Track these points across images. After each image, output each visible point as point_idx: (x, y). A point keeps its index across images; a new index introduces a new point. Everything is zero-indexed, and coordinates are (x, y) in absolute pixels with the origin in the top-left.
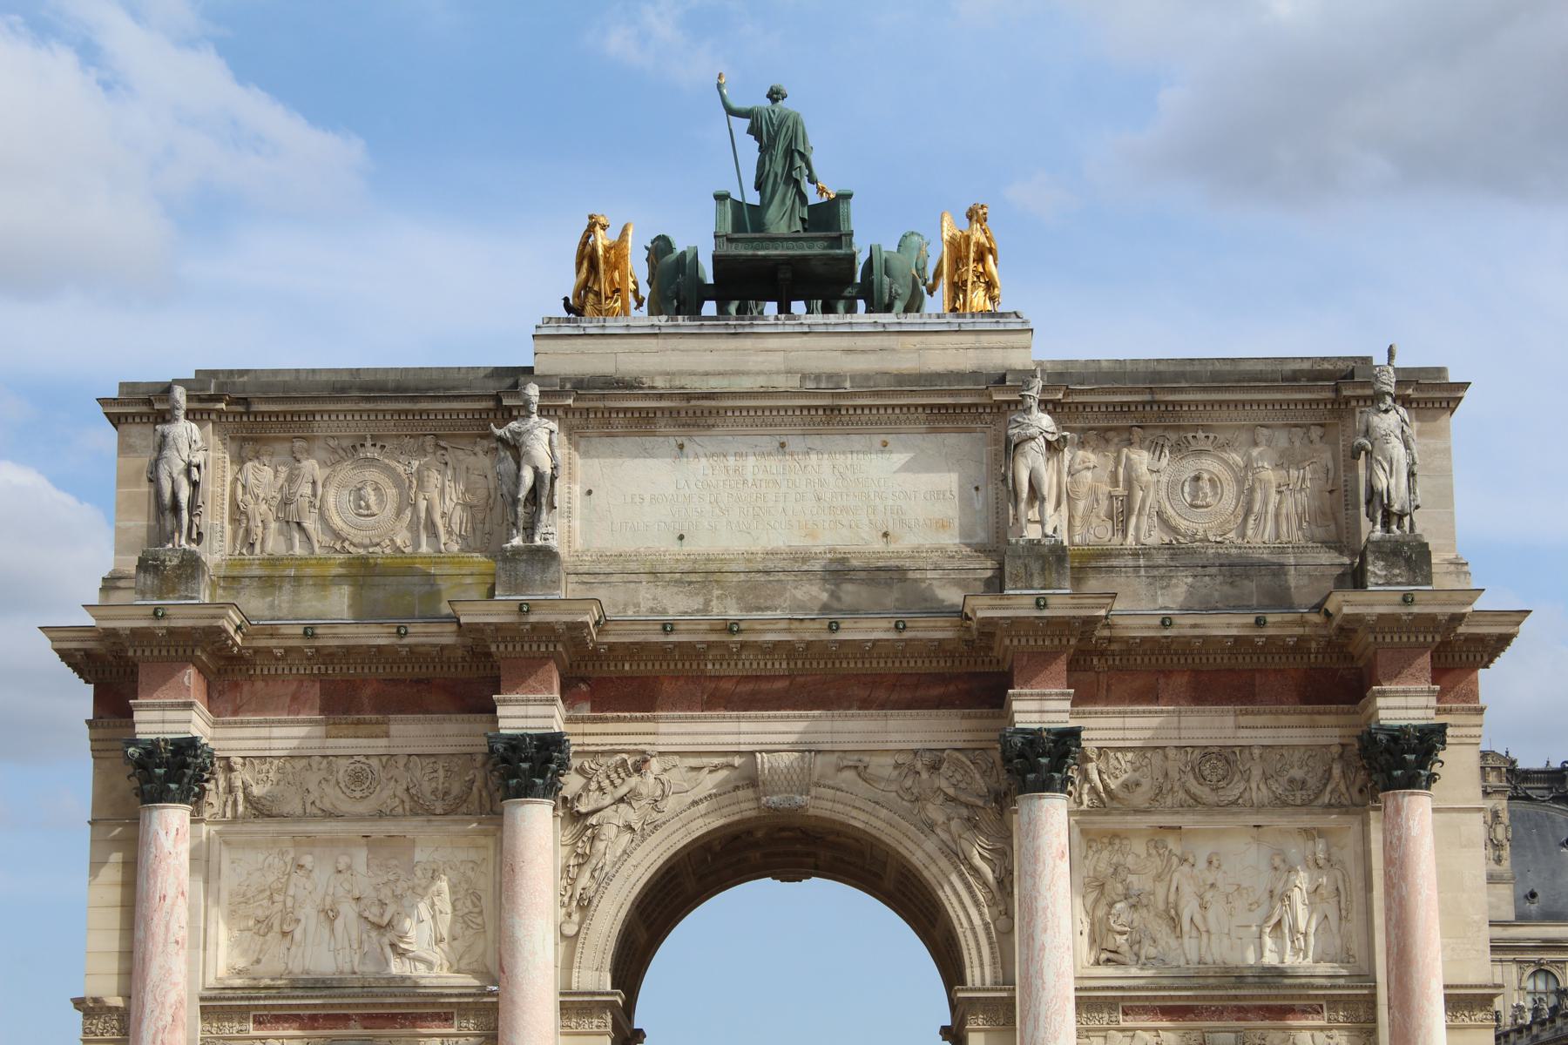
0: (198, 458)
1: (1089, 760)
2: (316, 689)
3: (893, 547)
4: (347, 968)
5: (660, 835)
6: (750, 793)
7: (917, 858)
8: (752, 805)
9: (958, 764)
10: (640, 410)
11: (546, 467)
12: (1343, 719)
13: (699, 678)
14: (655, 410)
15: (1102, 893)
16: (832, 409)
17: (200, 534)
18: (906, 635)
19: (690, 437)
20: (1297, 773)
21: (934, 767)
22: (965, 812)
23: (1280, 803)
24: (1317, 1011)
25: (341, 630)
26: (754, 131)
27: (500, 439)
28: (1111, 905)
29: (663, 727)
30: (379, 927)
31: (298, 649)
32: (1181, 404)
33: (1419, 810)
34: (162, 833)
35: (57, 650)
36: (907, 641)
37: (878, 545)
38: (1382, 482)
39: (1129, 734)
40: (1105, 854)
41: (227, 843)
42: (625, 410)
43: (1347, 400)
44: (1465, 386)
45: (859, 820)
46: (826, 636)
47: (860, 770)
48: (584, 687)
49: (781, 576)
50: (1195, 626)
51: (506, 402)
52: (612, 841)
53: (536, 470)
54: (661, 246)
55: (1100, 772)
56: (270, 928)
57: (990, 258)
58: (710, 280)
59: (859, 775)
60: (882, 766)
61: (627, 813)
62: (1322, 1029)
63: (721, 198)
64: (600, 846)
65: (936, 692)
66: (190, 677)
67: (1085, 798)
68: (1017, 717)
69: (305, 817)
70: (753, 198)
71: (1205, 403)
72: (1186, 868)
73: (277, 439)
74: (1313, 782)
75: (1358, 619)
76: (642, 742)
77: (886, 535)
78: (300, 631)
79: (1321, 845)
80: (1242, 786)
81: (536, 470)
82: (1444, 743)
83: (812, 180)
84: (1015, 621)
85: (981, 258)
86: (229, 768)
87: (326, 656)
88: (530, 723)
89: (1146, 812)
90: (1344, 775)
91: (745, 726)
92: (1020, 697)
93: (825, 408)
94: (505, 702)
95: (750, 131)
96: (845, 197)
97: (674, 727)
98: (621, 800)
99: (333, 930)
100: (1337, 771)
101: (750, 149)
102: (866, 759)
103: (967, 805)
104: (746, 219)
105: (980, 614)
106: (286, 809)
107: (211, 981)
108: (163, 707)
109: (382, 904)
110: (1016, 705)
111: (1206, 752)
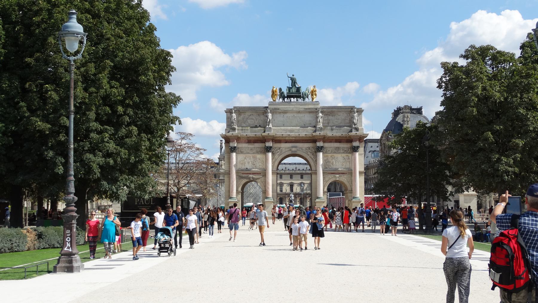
20: (346, 150)
23: (343, 153)
26: (291, 79)
33: (357, 154)
38: (355, 121)
47: (302, 149)
54: (280, 89)
58: (286, 96)
61: (278, 153)
63: (287, 87)
65: (309, 141)
79: (348, 157)
85: (315, 92)
96: (300, 87)
101: (290, 81)
104: (289, 89)
111: (336, 147)
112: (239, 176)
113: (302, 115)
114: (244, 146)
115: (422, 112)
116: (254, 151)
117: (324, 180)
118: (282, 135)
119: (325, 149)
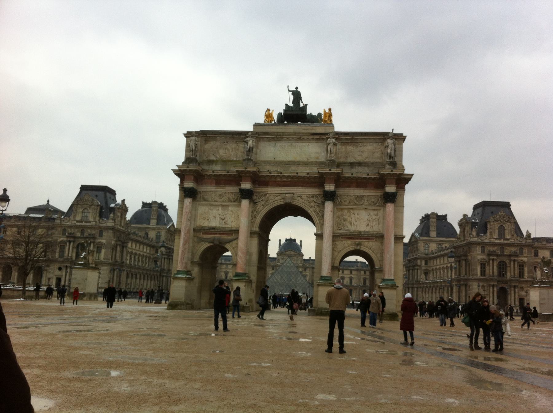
0: (197, 143)
1: (338, 196)
2: (214, 181)
3: (309, 161)
4: (217, 226)
5: (268, 206)
6: (283, 200)
7: (309, 212)
8: (283, 202)
9: (316, 197)
10: (269, 138)
11: (252, 146)
12: (381, 191)
13: (275, 182)
14: (271, 138)
15: (339, 218)
16: (300, 138)
17: (196, 155)
18: (309, 175)
19: (277, 142)
20: (373, 200)
21: (313, 197)
22: (317, 204)
23: (370, 205)
24: (373, 239)
25: (218, 171)
27: (245, 141)
28: (341, 220)
29: (269, 189)
30: (222, 219)
31: (212, 174)
32: (358, 138)
34: (187, 203)
35: (174, 173)
36: (310, 176)
37: (306, 160)
38: (389, 151)
39: (345, 193)
40: (340, 212)
41: (199, 205)
42: (266, 138)
43: (386, 138)
44: (406, 136)
45: (300, 205)
46: (296, 175)
48: (257, 182)
49: (290, 165)
50: (357, 175)
51: (247, 136)
52: (259, 207)
53: (250, 146)
55: (340, 199)
56: (205, 219)
57: (331, 117)
59: (301, 198)
60: (304, 197)
61: (263, 203)
62: (374, 242)
63: (286, 105)
64: (258, 208)
66: (192, 177)
67: (337, 203)
68: (325, 189)
69: (212, 201)
70: (292, 105)
71: (361, 138)
72: (353, 215)
73: (211, 141)
74: (375, 202)
75: (384, 173)
76: (266, 192)
77: (308, 159)
78: (212, 171)
79: (376, 212)
80: (363, 202)
81: (250, 146)
82: (397, 194)
83: (302, 102)
84: (326, 173)
86: (201, 193)
87: (216, 175)
88: (246, 187)
89: (347, 205)
90: (381, 200)
91: (282, 189)
92: (326, 185)
93: (299, 138)
94: (242, 184)
95: (292, 94)
96: (306, 105)
97: (271, 189)
98: (262, 201)
99: (215, 220)
100: (379, 200)
101: (292, 97)
102: (302, 195)
103: (318, 203)
105: (320, 171)
106: (209, 200)
107: (195, 227)
108: (188, 182)
109: (223, 215)
110: (325, 187)
112: (198, 237)
113: (304, 144)
114: (210, 189)
115: (447, 218)
116: (225, 198)
117: (336, 249)
118: (270, 173)
119: (339, 198)
